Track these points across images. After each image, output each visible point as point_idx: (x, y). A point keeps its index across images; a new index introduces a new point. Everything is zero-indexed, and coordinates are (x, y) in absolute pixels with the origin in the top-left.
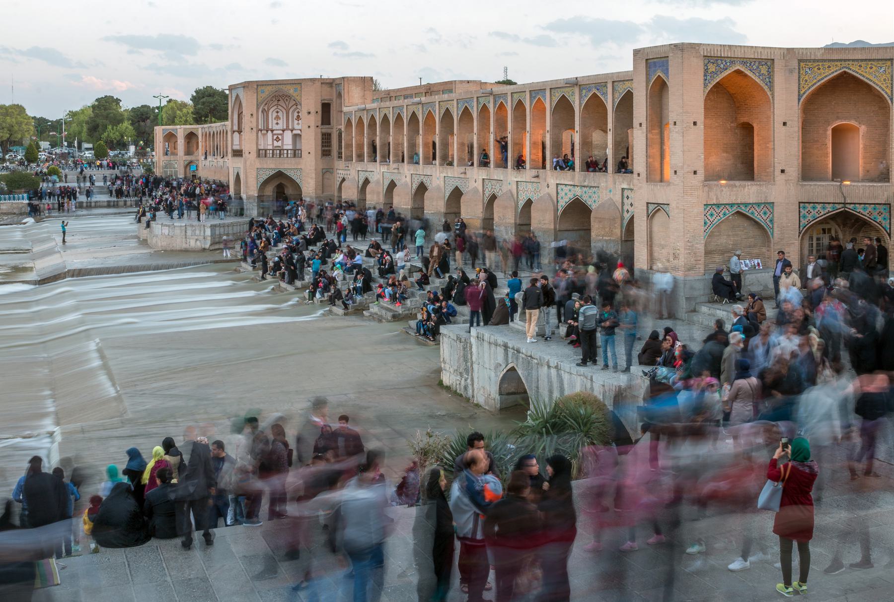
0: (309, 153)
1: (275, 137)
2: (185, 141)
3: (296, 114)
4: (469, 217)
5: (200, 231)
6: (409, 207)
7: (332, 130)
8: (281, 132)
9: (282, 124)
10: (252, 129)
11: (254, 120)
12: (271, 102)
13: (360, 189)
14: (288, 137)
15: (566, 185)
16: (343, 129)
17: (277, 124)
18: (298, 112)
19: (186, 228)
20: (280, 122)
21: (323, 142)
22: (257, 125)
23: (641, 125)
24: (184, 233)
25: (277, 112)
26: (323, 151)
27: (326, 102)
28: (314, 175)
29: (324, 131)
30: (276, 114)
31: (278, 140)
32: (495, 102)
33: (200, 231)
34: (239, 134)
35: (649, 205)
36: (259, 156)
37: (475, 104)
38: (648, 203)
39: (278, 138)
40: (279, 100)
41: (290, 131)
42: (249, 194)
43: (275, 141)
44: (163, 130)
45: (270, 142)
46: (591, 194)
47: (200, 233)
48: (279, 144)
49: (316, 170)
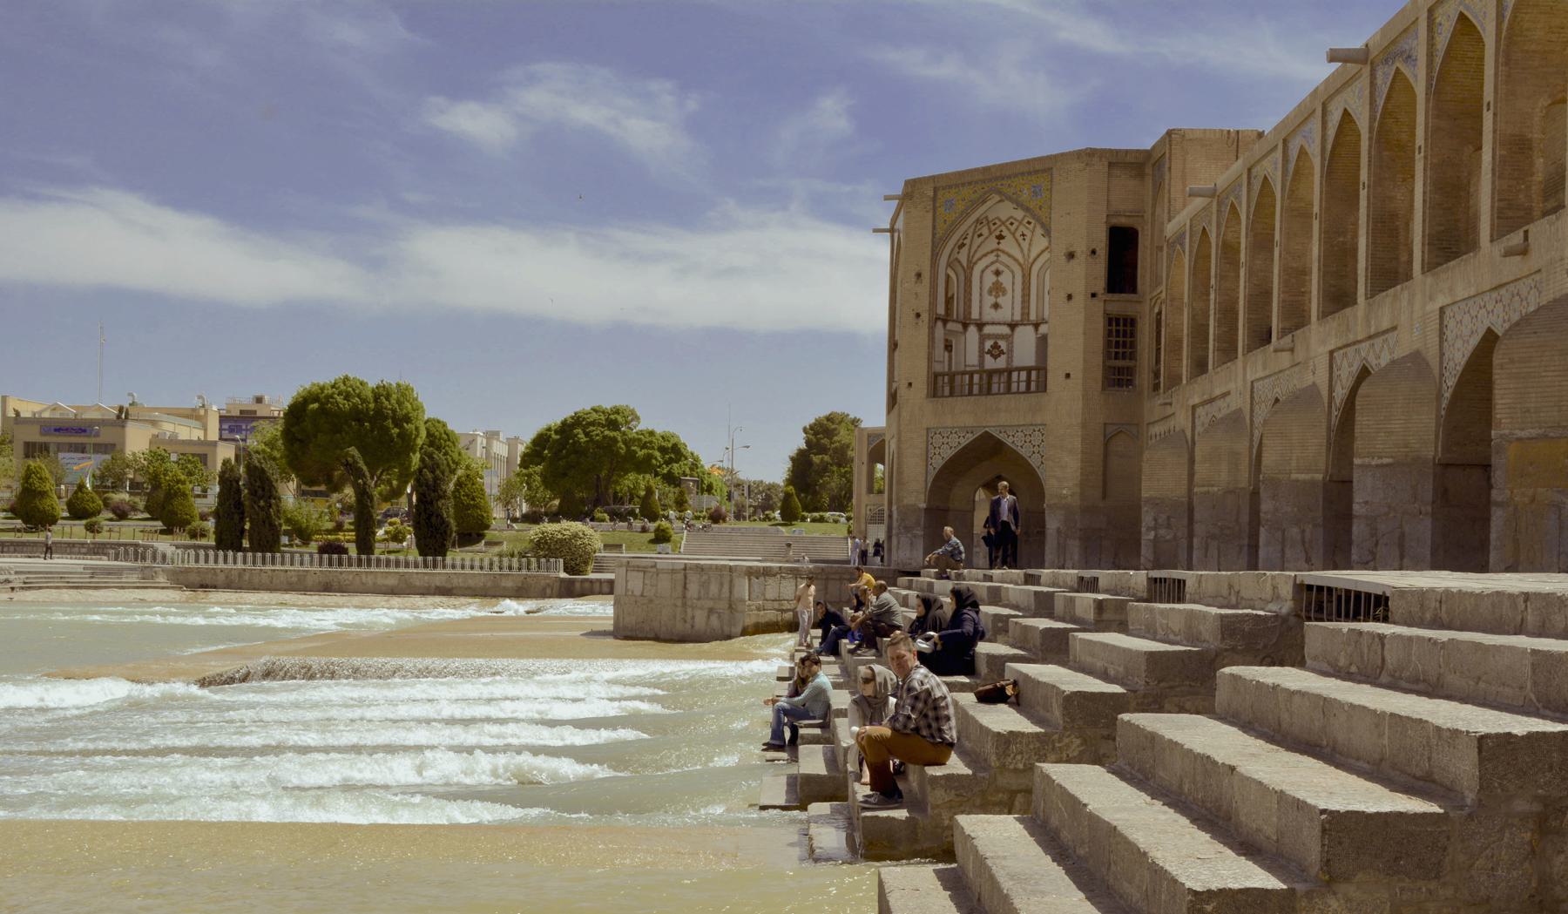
0: (1068, 376)
1: (988, 344)
4: (1534, 432)
5: (722, 584)
6: (1319, 477)
8: (1006, 330)
9: (1010, 308)
10: (918, 315)
11: (924, 289)
12: (978, 241)
14: (1025, 341)
17: (996, 306)
19: (685, 577)
21: (1108, 344)
24: (680, 588)
25: (998, 273)
27: (1123, 221)
28: (1078, 443)
30: (994, 278)
31: (996, 352)
33: (722, 584)
36: (934, 392)
39: (996, 346)
40: (1000, 237)
41: (1030, 329)
42: (906, 502)
43: (988, 357)
45: (972, 359)
47: (720, 590)
49: (1084, 426)
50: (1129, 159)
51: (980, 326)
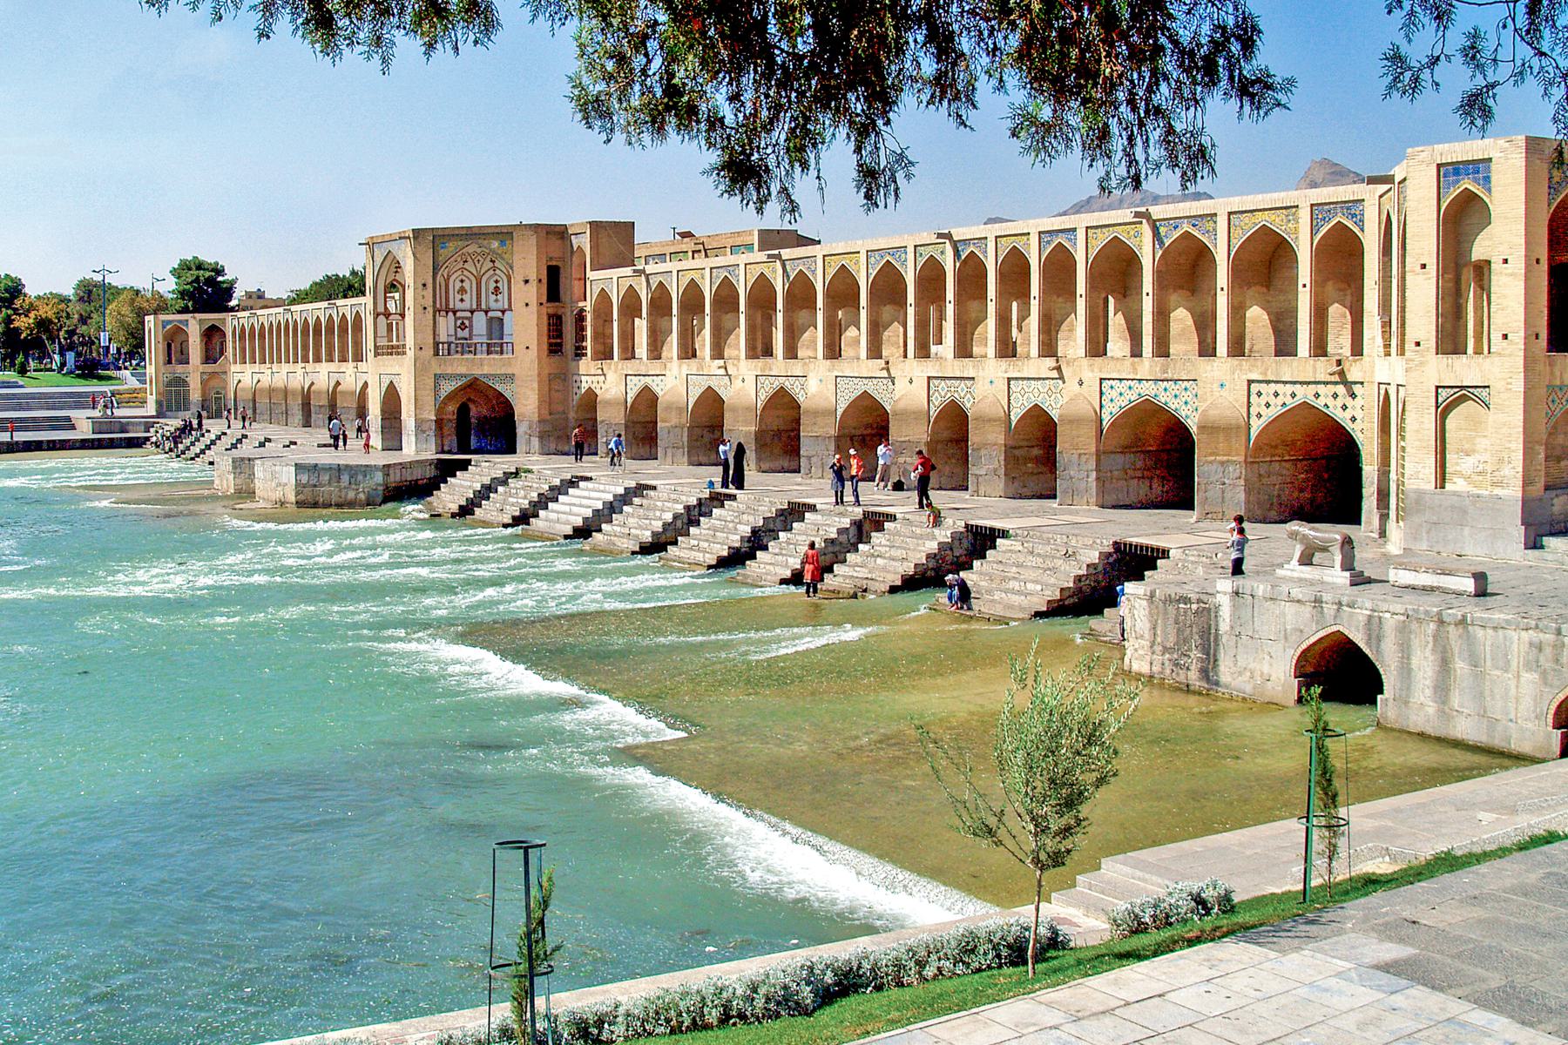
1: (459, 322)
2: (202, 341)
3: (493, 285)
7: (563, 310)
8: (469, 314)
9: (469, 301)
10: (425, 308)
13: (629, 405)
14: (480, 321)
15: (1120, 380)
16: (588, 309)
17: (462, 300)
18: (497, 282)
20: (466, 297)
22: (435, 302)
23: (1424, 266)
25: (462, 281)
26: (550, 345)
27: (554, 263)
28: (535, 385)
29: (551, 311)
32: (957, 253)
34: (387, 318)
35: (1440, 390)
37: (911, 256)
38: (1437, 387)
39: (463, 323)
40: (466, 261)
41: (483, 313)
44: (163, 321)
46: (1183, 393)
48: (466, 333)
49: (539, 375)
50: (557, 229)
51: (455, 313)
